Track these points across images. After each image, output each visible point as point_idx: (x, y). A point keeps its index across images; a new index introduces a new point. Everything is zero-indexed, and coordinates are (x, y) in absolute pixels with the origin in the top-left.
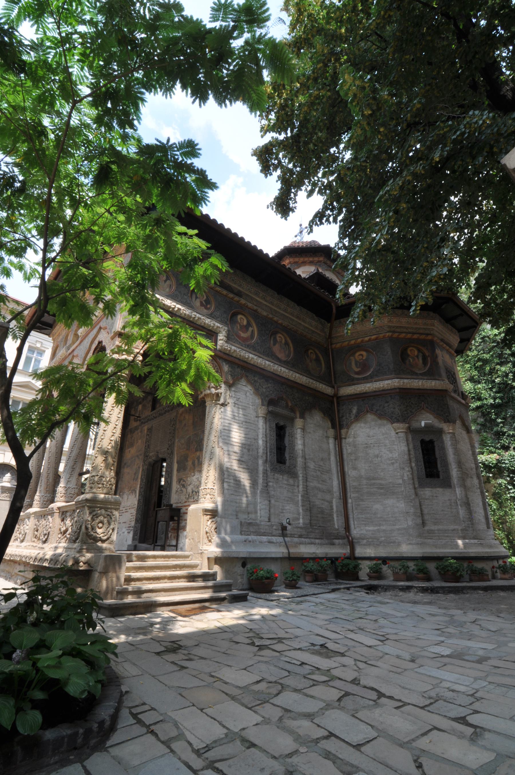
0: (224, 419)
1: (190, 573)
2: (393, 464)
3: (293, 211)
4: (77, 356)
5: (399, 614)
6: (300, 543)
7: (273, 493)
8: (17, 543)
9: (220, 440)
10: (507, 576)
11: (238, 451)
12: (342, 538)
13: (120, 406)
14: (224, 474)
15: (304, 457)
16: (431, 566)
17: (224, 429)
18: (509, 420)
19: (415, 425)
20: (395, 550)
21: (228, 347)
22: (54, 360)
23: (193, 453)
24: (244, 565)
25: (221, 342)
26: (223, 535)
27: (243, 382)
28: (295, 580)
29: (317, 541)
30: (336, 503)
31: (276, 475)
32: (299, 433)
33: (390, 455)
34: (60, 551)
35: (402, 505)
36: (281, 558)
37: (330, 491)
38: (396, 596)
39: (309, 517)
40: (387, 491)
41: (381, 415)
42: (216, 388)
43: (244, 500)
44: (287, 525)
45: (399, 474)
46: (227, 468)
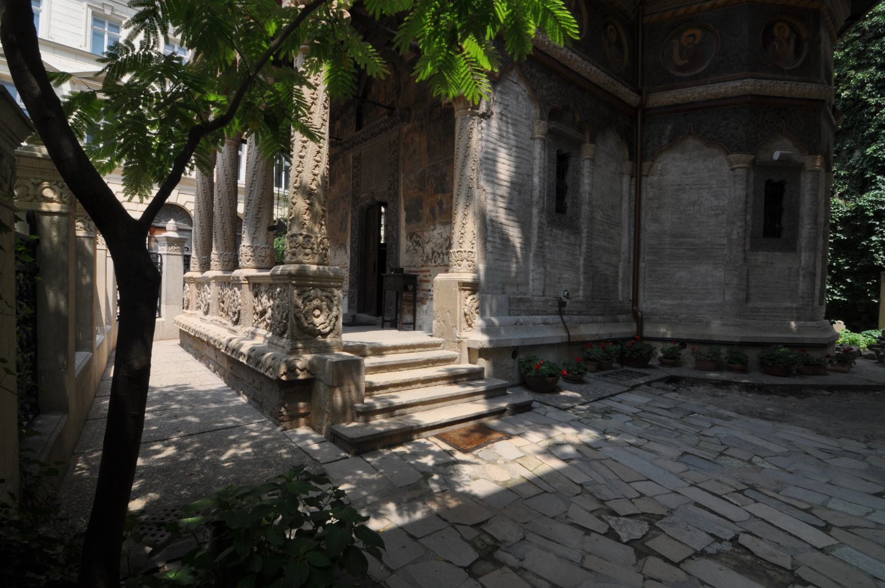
0: (487, 141)
2: (717, 215)
6: (581, 323)
7: (548, 256)
9: (482, 176)
11: (505, 195)
14: (489, 230)
16: (752, 355)
17: (487, 158)
18: (843, 154)
23: (437, 196)
26: (488, 316)
28: (580, 373)
29: (600, 318)
30: (623, 269)
31: (554, 230)
33: (715, 203)
34: (259, 341)
35: (720, 274)
43: (514, 267)
45: (723, 230)
46: (492, 220)
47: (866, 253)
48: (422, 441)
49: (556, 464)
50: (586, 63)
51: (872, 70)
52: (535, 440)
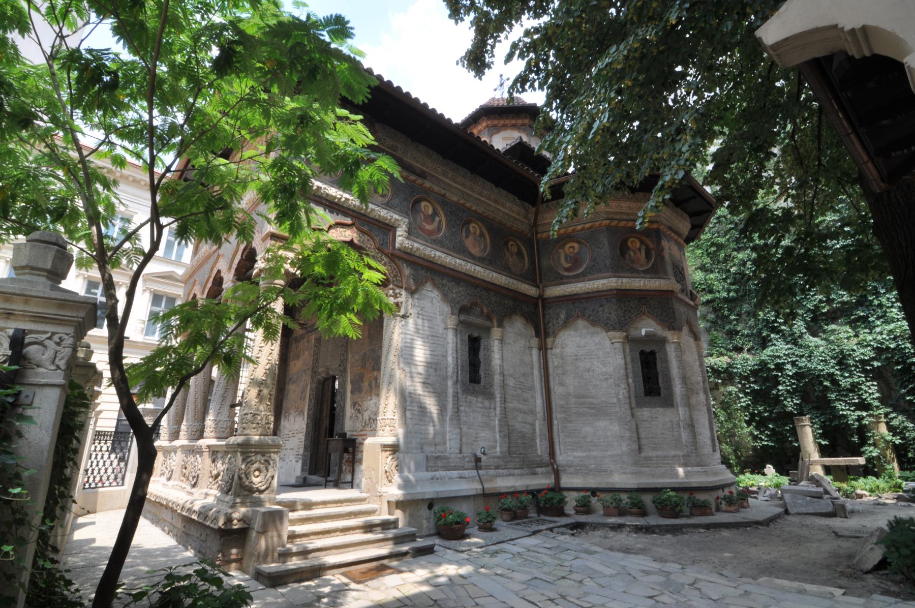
0: (406, 334)
1: (366, 522)
2: (606, 379)
3: (489, 67)
4: (223, 255)
5: (608, 571)
8: (164, 479)
10: (732, 508)
12: (546, 465)
13: (270, 343)
14: (406, 400)
15: (502, 374)
16: (647, 499)
18: (744, 316)
19: (633, 333)
20: (606, 480)
21: (408, 244)
22: (196, 258)
24: (430, 506)
25: (400, 238)
26: (406, 473)
27: (429, 286)
28: (490, 522)
29: (517, 471)
30: (539, 426)
32: (496, 345)
33: (604, 369)
34: (210, 500)
35: (615, 428)
36: (474, 496)
37: (532, 412)
38: (605, 538)
39: (507, 445)
40: (599, 411)
41: (595, 321)
42: (395, 296)
43: (431, 430)
44: (482, 456)
46: (410, 393)
47: (777, 401)
48: (328, 577)
49: (425, 588)
50: (488, 271)
51: (748, 251)
52: (422, 573)
